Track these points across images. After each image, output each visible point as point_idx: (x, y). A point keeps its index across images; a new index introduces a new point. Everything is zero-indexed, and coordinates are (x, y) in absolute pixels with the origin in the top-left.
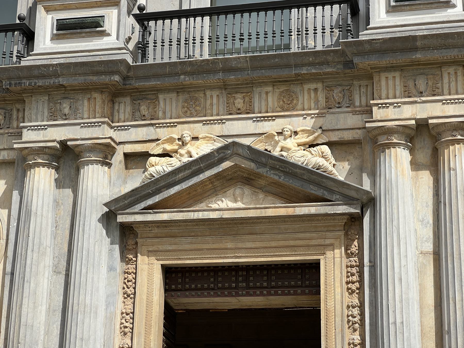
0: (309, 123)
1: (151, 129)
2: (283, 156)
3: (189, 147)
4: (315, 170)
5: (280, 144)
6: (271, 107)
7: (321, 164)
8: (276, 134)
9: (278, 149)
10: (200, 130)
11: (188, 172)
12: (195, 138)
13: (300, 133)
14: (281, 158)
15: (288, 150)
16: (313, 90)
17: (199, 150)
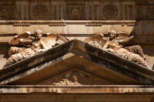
0: (129, 30)
1: (11, 26)
2: (110, 51)
3: (41, 42)
4: (133, 62)
5: (108, 43)
6: (99, 16)
7: (137, 59)
8: (103, 35)
9: (106, 46)
10: (48, 29)
11: (42, 59)
12: (45, 35)
13: (119, 35)
14: (110, 53)
15: (113, 47)
16: (129, 6)
17: (47, 43)
